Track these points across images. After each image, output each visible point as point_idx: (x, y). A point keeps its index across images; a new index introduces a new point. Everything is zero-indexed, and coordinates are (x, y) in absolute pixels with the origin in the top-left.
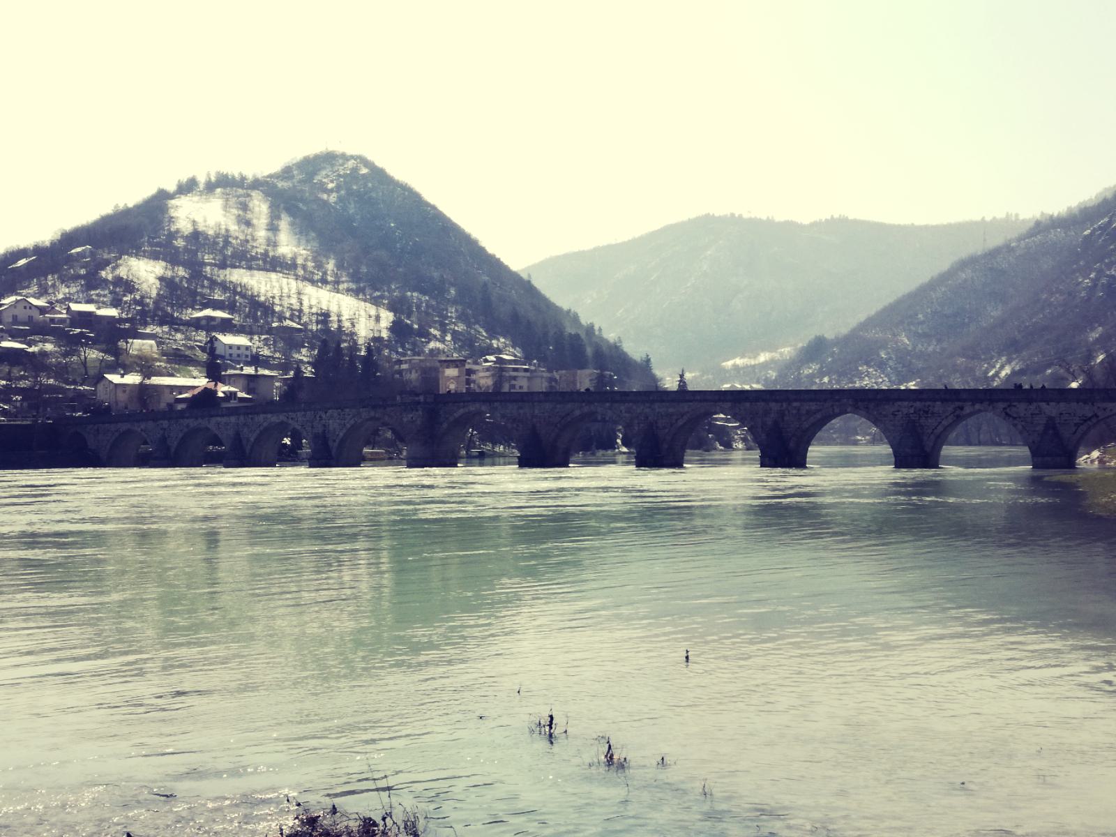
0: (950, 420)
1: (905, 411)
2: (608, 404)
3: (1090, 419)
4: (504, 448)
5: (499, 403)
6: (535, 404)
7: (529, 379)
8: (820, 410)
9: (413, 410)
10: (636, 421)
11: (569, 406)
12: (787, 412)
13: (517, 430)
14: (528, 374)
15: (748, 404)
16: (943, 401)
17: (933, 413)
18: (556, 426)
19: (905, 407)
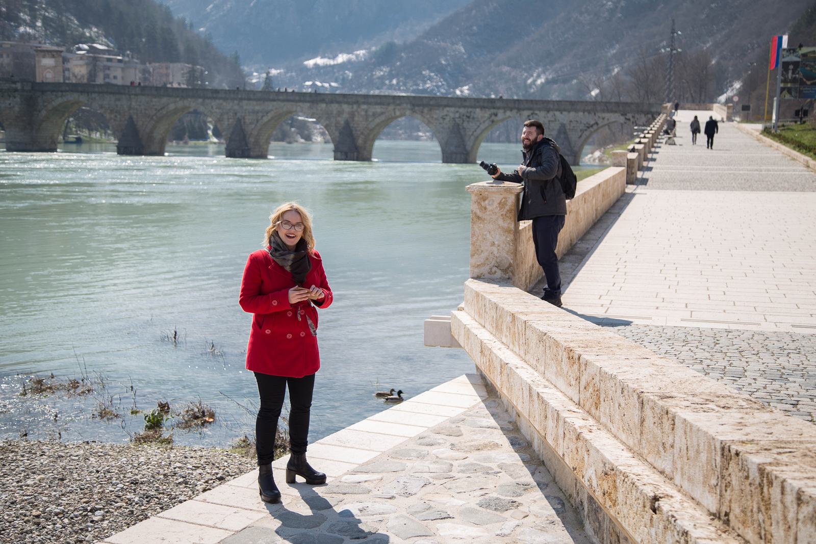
0: (486, 124)
1: (452, 115)
2: (200, 100)
3: (592, 126)
4: (101, 135)
5: (96, 95)
6: (132, 96)
7: (123, 69)
8: (382, 113)
9: (10, 96)
10: (225, 117)
11: (165, 100)
12: (356, 113)
13: (115, 120)
14: (122, 65)
15: (324, 105)
16: (483, 108)
17: (473, 118)
18: (152, 118)
19: (451, 112)
